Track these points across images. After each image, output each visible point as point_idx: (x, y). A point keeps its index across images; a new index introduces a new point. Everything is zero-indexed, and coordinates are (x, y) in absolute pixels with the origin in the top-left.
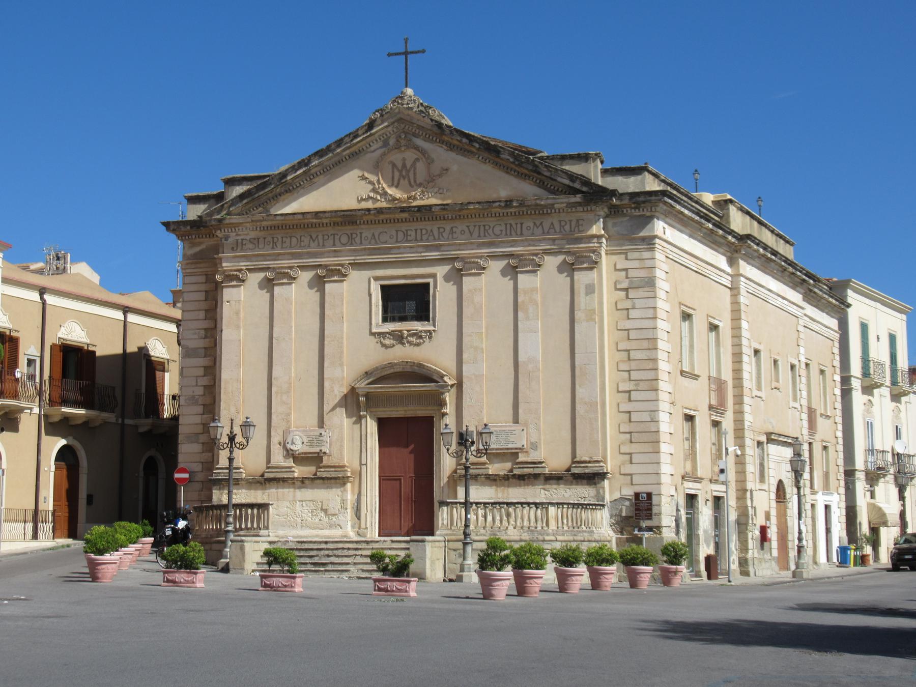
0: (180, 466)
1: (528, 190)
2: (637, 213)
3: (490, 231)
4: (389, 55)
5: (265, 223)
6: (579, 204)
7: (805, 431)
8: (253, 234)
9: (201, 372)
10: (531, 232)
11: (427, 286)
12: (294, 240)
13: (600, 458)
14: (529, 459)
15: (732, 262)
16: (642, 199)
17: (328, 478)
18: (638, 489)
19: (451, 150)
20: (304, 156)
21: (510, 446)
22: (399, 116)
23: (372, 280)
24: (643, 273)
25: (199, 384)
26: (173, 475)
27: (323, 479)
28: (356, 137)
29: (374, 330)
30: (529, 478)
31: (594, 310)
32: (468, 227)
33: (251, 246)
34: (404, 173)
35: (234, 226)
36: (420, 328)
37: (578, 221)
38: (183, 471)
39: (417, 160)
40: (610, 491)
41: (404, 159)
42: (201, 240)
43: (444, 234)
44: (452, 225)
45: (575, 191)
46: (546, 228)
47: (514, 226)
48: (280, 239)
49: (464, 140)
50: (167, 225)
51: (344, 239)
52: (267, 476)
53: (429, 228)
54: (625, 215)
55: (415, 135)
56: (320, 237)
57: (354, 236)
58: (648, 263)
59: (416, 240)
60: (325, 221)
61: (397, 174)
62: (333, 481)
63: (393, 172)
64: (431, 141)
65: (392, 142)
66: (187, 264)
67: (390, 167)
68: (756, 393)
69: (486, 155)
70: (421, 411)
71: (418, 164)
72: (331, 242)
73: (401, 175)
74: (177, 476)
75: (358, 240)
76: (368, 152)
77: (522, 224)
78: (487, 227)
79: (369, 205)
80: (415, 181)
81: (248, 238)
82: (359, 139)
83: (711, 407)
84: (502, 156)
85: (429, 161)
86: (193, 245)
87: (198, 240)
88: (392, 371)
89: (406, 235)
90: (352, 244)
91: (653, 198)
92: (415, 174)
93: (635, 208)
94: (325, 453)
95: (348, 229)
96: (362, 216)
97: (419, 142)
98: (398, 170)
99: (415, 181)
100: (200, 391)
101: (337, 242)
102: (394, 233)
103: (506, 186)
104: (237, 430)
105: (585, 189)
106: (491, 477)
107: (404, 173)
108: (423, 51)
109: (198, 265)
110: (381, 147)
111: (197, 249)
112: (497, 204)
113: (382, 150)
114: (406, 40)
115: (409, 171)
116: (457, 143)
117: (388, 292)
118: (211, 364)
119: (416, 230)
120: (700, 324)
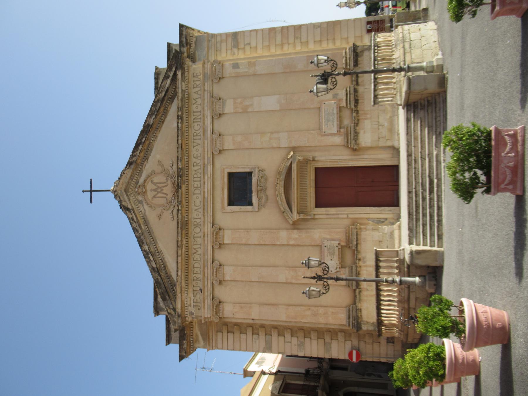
0: (347, 358)
1: (173, 110)
2: (193, 45)
3: (197, 132)
4: (91, 202)
5: (183, 284)
6: (183, 74)
8: (191, 295)
9: (281, 338)
10: (199, 106)
11: (230, 175)
12: (196, 265)
13: (344, 51)
14: (344, 98)
16: (184, 40)
17: (357, 240)
18: (365, 31)
19: (147, 159)
20: (141, 254)
21: (335, 112)
22: (123, 191)
23: (224, 211)
24: (230, 40)
25: (290, 341)
26: (354, 363)
27: (357, 244)
28: (133, 219)
29: (257, 209)
30: (357, 96)
31: (249, 62)
32: (194, 147)
34: (159, 190)
35: (183, 306)
36: (256, 177)
37: (194, 77)
38: (350, 354)
39: (152, 182)
40: (366, 40)
41: (151, 190)
42: (194, 334)
43: (198, 162)
44: (192, 157)
45: (175, 74)
46: (198, 96)
47: (195, 117)
48: (195, 275)
49: (140, 147)
50: (181, 358)
51: (197, 230)
53: (193, 173)
54: (194, 53)
55: (137, 183)
56: (195, 247)
57: (195, 223)
58: (224, 37)
59: (200, 181)
60: (184, 242)
61: (160, 195)
62: (359, 237)
64: (141, 171)
65: (140, 198)
66: (209, 345)
67: (155, 199)
69: (151, 134)
70: (311, 176)
71: (155, 181)
72: (198, 239)
73: (160, 192)
74: (354, 360)
75: (198, 221)
76: (145, 214)
77: (194, 112)
78: (195, 134)
80: (165, 183)
81: (193, 298)
82: (135, 218)
84: (151, 123)
85: (154, 173)
86: (197, 340)
87: (194, 337)
88: (283, 195)
89: (196, 188)
90: (200, 225)
91: (184, 33)
92: (160, 183)
93: (190, 46)
94: (339, 244)
95: (191, 227)
96: (182, 216)
97: (141, 180)
98: (158, 193)
99: (165, 183)
100: (295, 340)
101: (199, 235)
102: (195, 196)
103: (171, 122)
105: (174, 69)
106: (356, 122)
107: (159, 190)
108: (91, 180)
109: (211, 337)
110: (143, 205)
111: (200, 338)
112: (179, 125)
113: (145, 204)
114: (84, 191)
115: (158, 187)
116: (142, 154)
118: (276, 330)
119: (194, 181)
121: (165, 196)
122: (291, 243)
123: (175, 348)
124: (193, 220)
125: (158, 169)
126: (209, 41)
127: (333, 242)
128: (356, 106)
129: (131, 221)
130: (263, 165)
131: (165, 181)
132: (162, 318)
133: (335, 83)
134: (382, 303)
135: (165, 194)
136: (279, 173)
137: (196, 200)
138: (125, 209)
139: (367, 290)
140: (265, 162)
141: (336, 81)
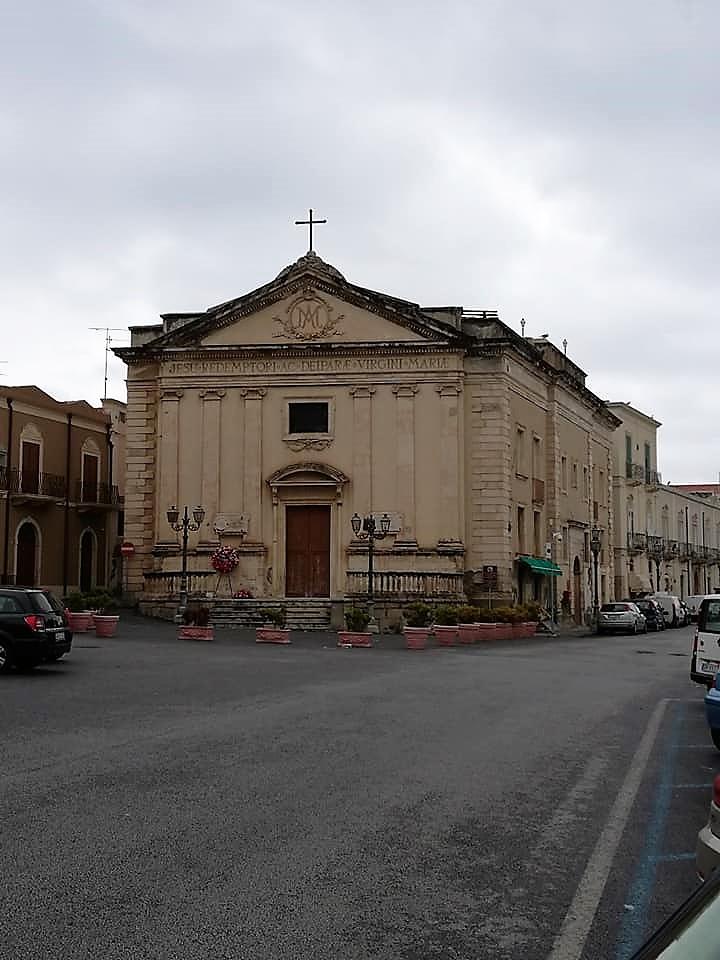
7: (592, 520)
9: (143, 467)
15: (550, 392)
30: (404, 555)
33: (186, 370)
34: (309, 316)
38: (130, 545)
45: (443, 337)
52: (198, 549)
59: (318, 370)
68: (562, 491)
79: (283, 341)
83: (533, 501)
92: (317, 317)
97: (320, 294)
104: (190, 516)
105: (451, 335)
107: (309, 316)
115: (311, 316)
117: (295, 409)
120: (528, 438)
122: (246, 479)
123: (125, 341)
124: (272, 362)
125: (334, 316)
127: (246, 527)
128: (393, 553)
129: (271, 285)
130: (334, 446)
132: (160, 321)
136: (322, 467)
137: (296, 367)
138: (283, 278)
139: (196, 563)
140: (339, 449)
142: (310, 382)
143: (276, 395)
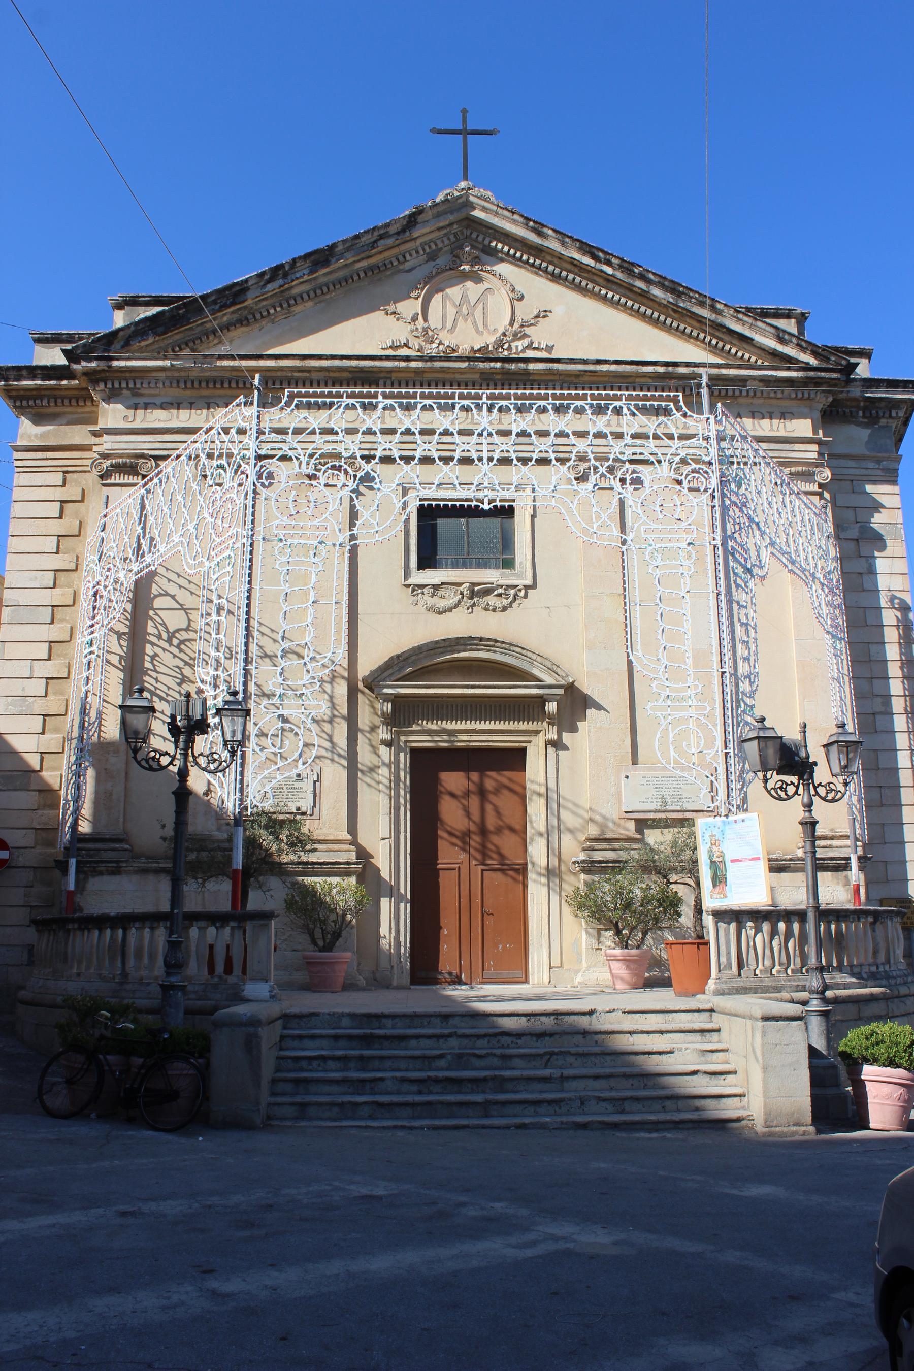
63: (444, 307)
76: (400, 271)
98: (454, 304)
107: (464, 310)
114: (464, 112)
121: (449, 325)
125: (525, 312)
126: (879, 461)
131: (491, 328)
133: (782, 794)
134: (147, 932)
135: (454, 326)
136: (509, 646)
141: (789, 798)
142: (473, 451)
143: (389, 478)
